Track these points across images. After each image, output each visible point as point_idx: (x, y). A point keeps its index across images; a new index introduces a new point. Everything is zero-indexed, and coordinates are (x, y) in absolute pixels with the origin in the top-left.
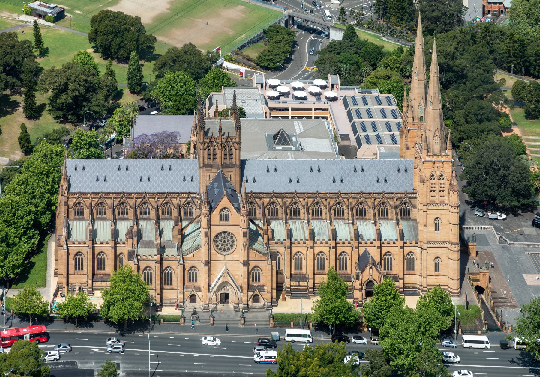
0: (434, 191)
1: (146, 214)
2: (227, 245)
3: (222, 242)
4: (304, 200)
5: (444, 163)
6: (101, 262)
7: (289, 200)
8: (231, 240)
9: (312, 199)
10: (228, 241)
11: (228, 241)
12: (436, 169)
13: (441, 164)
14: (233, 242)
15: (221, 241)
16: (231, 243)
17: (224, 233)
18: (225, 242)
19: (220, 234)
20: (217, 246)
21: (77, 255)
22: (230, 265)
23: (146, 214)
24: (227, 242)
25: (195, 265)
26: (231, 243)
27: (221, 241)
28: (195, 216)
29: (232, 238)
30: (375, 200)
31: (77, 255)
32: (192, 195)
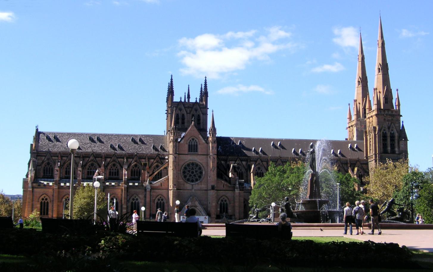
1: (115, 175)
2: (195, 176)
3: (190, 173)
8: (199, 171)
14: (201, 173)
15: (189, 171)
18: (193, 172)
20: (185, 177)
23: (115, 175)
24: (195, 173)
27: (189, 171)
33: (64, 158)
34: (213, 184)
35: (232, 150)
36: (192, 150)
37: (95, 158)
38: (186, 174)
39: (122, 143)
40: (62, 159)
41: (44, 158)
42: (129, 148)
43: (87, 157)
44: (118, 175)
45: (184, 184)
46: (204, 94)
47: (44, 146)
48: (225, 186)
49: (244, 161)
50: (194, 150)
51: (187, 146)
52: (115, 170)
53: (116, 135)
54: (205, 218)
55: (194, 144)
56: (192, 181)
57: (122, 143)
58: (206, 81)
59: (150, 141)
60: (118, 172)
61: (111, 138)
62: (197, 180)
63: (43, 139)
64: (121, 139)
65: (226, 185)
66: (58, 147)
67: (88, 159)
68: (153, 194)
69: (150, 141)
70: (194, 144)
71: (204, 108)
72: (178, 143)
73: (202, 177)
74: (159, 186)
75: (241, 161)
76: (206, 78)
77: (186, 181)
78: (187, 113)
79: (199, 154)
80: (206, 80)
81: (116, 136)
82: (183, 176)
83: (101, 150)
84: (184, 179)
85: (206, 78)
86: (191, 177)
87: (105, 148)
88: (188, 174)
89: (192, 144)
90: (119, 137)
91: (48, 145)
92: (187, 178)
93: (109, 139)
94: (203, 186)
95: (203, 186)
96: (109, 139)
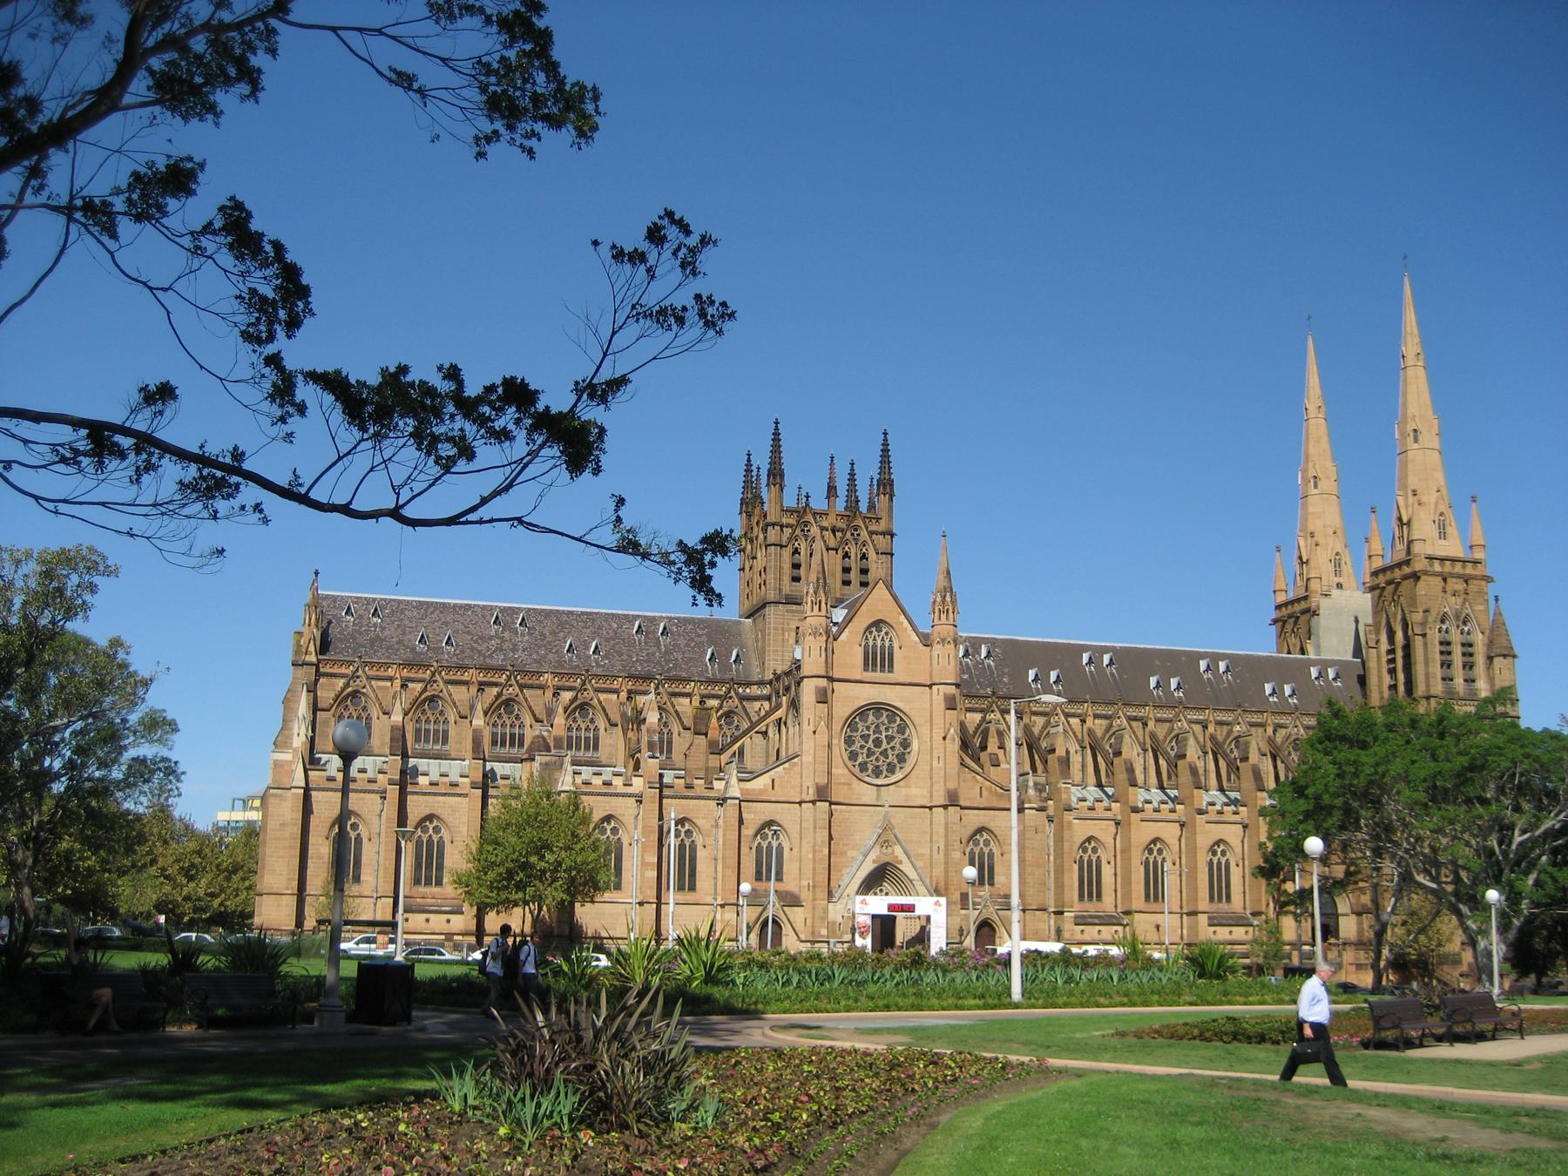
1: (587, 748)
2: (884, 753)
3: (870, 744)
4: (1083, 721)
6: (429, 856)
9: (1105, 722)
10: (890, 739)
14: (906, 744)
15: (865, 738)
17: (878, 708)
18: (877, 743)
19: (862, 712)
20: (853, 756)
23: (587, 748)
29: (901, 730)
30: (1275, 731)
34: (952, 785)
37: (522, 687)
38: (856, 747)
40: (404, 686)
41: (341, 682)
43: (495, 684)
44: (596, 748)
45: (849, 784)
46: (885, 485)
48: (985, 793)
50: (882, 666)
54: (937, 903)
55: (883, 647)
56: (877, 772)
60: (596, 739)
62: (891, 769)
64: (600, 628)
65: (990, 790)
66: (391, 647)
67: (495, 690)
70: (883, 647)
71: (883, 534)
73: (911, 760)
77: (857, 770)
79: (902, 680)
80: (886, 440)
84: (850, 764)
87: (550, 656)
89: (875, 646)
91: (354, 638)
92: (860, 760)
93: (562, 624)
94: (914, 791)
95: (914, 791)
96: (562, 624)
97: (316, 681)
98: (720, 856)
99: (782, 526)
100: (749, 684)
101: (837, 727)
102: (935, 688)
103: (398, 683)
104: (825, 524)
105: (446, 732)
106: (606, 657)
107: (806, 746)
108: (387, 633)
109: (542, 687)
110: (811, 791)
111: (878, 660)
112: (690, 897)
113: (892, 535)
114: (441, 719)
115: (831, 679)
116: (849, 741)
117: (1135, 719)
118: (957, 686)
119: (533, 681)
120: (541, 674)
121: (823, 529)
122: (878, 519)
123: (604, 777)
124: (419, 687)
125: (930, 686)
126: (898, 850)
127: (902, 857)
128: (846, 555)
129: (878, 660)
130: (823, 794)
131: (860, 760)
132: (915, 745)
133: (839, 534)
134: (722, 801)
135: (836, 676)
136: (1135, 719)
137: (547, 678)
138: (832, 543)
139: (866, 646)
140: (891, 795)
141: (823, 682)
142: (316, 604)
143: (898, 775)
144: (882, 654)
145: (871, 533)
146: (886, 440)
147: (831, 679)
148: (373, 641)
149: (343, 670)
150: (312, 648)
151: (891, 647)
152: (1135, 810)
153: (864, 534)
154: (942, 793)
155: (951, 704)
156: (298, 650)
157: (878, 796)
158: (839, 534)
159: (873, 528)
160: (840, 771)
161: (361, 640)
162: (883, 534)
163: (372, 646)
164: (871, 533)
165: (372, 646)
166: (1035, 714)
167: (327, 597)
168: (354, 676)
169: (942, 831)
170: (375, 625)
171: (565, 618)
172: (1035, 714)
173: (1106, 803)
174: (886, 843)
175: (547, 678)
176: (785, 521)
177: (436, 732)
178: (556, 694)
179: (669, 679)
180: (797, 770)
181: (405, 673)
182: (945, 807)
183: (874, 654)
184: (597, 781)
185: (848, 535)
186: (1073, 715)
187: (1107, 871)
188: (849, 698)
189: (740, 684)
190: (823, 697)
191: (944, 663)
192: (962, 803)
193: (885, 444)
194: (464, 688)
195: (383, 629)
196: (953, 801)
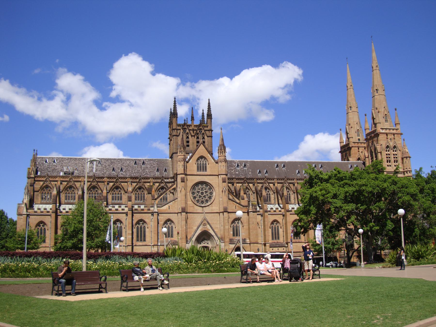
0: (390, 166)
1: (118, 200)
2: (205, 196)
3: (200, 194)
4: (274, 185)
5: (395, 135)
7: (260, 185)
8: (209, 191)
9: (281, 185)
10: (206, 192)
11: (206, 192)
12: (389, 140)
13: (393, 136)
14: (211, 193)
15: (198, 192)
16: (209, 195)
17: (202, 183)
18: (202, 193)
19: (197, 184)
20: (195, 198)
21: (40, 226)
22: (208, 217)
25: (171, 218)
26: (209, 195)
28: (168, 200)
29: (210, 189)
31: (40, 226)
32: (166, 180)
33: (63, 183)
34: (225, 205)
35: (237, 173)
36: (201, 170)
39: (125, 167)
41: (42, 183)
42: (132, 171)
44: (121, 199)
47: (43, 170)
48: (237, 207)
49: (251, 183)
50: (203, 170)
51: (195, 166)
52: (118, 194)
53: (119, 159)
55: (203, 164)
56: (202, 202)
57: (125, 167)
58: (209, 103)
59: (154, 164)
61: (113, 162)
62: (207, 201)
63: (42, 163)
64: (123, 163)
66: (58, 172)
68: (161, 218)
69: (154, 164)
70: (203, 164)
71: (209, 130)
72: (186, 162)
73: (213, 198)
74: (167, 210)
75: (248, 183)
76: (209, 100)
77: (196, 202)
78: (192, 136)
79: (209, 174)
80: (209, 102)
81: (119, 160)
82: (192, 198)
83: (103, 174)
84: (193, 200)
85: (209, 100)
86: (201, 198)
88: (197, 195)
89: (200, 164)
90: (122, 161)
91: (47, 169)
93: (112, 163)
95: (214, 208)
96: (112, 163)
97: (34, 183)
98: (153, 230)
99: (177, 130)
100: (168, 178)
101: (189, 189)
102: (219, 176)
103: (59, 182)
104: (190, 128)
105: (75, 196)
106: (125, 172)
107: (178, 196)
108: (57, 167)
109: (103, 182)
110: (181, 209)
111: (202, 168)
112: (144, 243)
113: (212, 131)
114: (73, 193)
115: (186, 175)
116: (193, 193)
117: (291, 183)
118: (226, 175)
119: (101, 180)
120: (103, 178)
121: (190, 130)
122: (207, 126)
123: (122, 208)
124: (66, 183)
125: (218, 175)
126: (208, 226)
127: (210, 228)
128: (198, 138)
129: (202, 168)
130: (184, 210)
131: (197, 199)
132: (214, 194)
133: (195, 132)
134: (153, 213)
135: (188, 173)
136: (291, 183)
137: (105, 179)
138: (193, 134)
139: (198, 164)
140: (206, 210)
141: (183, 176)
142: (34, 160)
143: (209, 203)
144: (203, 166)
145: (205, 131)
146: (209, 102)
147: (186, 175)
148: (53, 170)
149: (43, 179)
150: (33, 173)
151: (206, 164)
152: (288, 211)
153: (203, 131)
154: (222, 208)
155: (224, 181)
156: (29, 173)
157: (203, 210)
158: (195, 132)
159: (206, 129)
160: (190, 203)
161: (49, 170)
162: (209, 130)
163: (53, 171)
164: (205, 131)
165: (53, 171)
166: (259, 183)
167: (40, 158)
168: (46, 181)
169: (223, 220)
170: (54, 165)
171: (113, 161)
172: (259, 183)
173: (280, 209)
174: (205, 225)
175: (105, 179)
176: (178, 128)
177: (72, 196)
178: (108, 184)
179: (142, 178)
180: (177, 203)
181: (62, 179)
182: (223, 212)
183: (200, 166)
184: (113, 209)
185: (198, 131)
186: (271, 183)
187: (281, 231)
188: (192, 180)
189: (165, 178)
190: (183, 181)
191: (222, 168)
192: (229, 211)
193: (209, 103)
194: (79, 183)
195: (56, 166)
196: (225, 211)
